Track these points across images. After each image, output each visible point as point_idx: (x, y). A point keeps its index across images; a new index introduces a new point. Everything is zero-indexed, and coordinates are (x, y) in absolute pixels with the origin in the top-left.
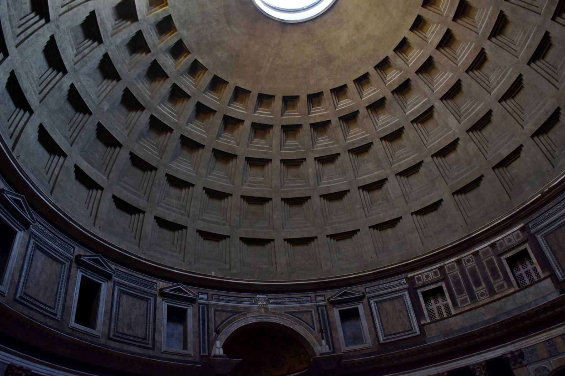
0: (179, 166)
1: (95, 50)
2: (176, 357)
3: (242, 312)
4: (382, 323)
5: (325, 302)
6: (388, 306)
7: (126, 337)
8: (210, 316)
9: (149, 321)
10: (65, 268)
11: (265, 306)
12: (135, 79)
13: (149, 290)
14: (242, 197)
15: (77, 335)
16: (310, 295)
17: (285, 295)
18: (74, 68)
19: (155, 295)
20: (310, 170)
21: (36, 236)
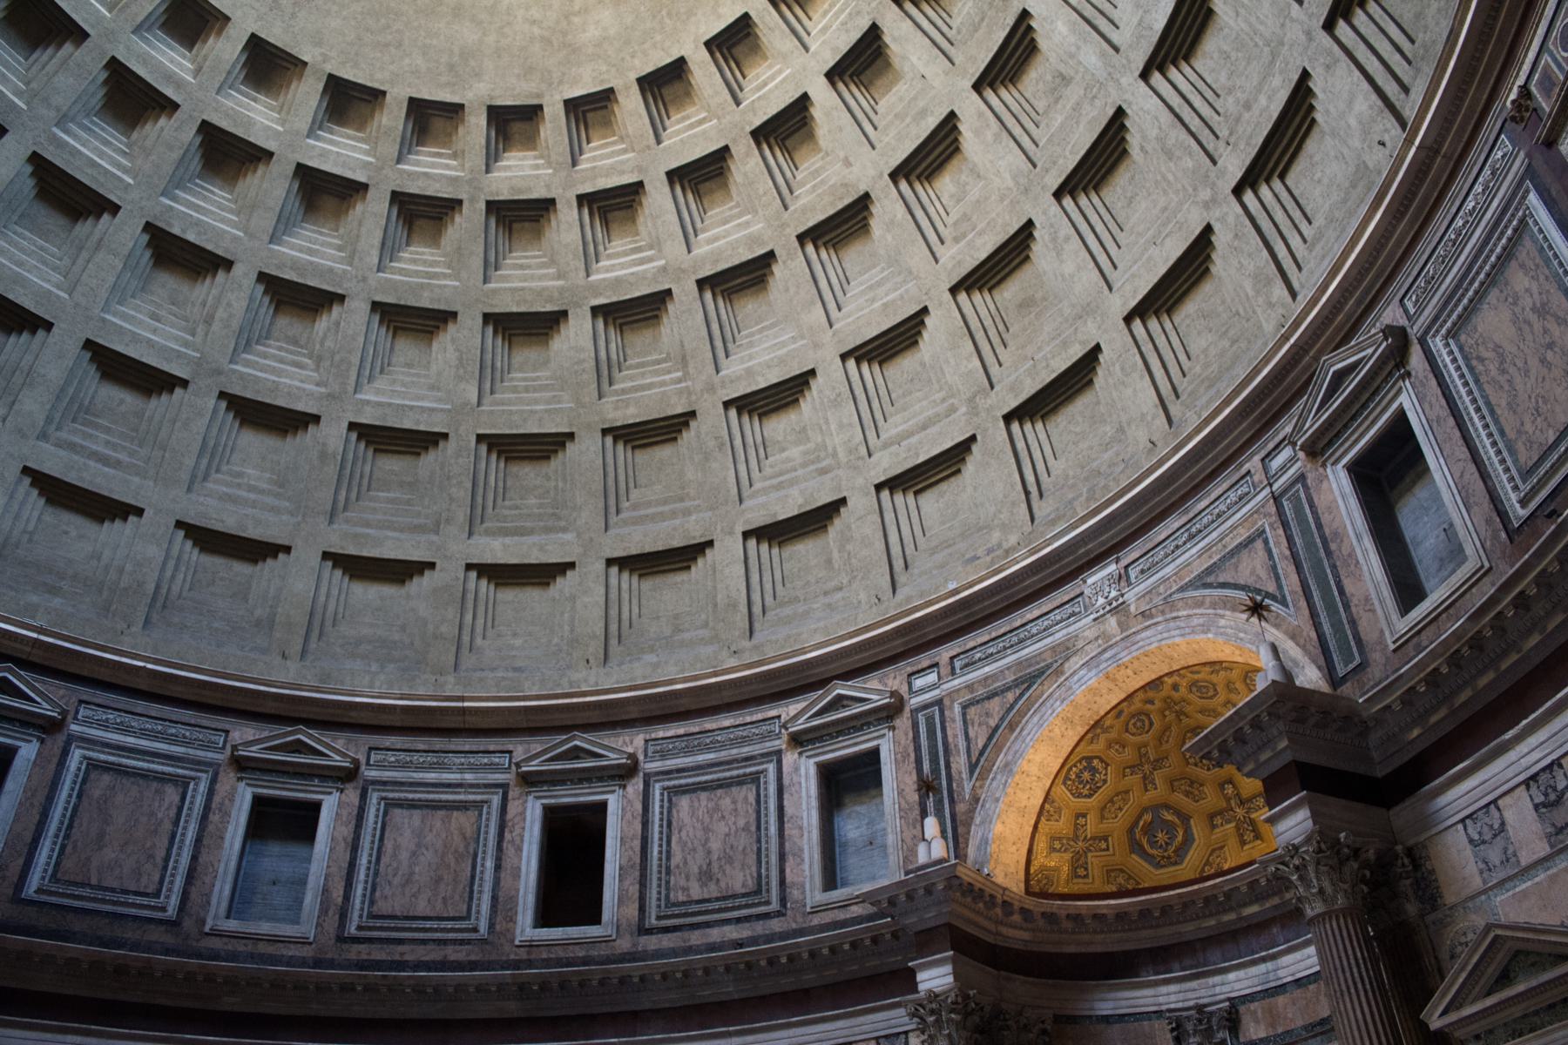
0: (751, 357)
1: (342, 324)
2: (856, 910)
3: (1048, 666)
4: (1496, 421)
5: (1299, 464)
6: (1494, 321)
7: (695, 908)
8: (949, 733)
9: (767, 835)
10: (488, 813)
11: (1115, 604)
12: (486, 280)
13: (757, 747)
14: (954, 290)
15: (544, 956)
16: (1243, 470)
17: (1173, 523)
18: (329, 395)
19: (779, 753)
20: (1061, 27)
21: (385, 783)
